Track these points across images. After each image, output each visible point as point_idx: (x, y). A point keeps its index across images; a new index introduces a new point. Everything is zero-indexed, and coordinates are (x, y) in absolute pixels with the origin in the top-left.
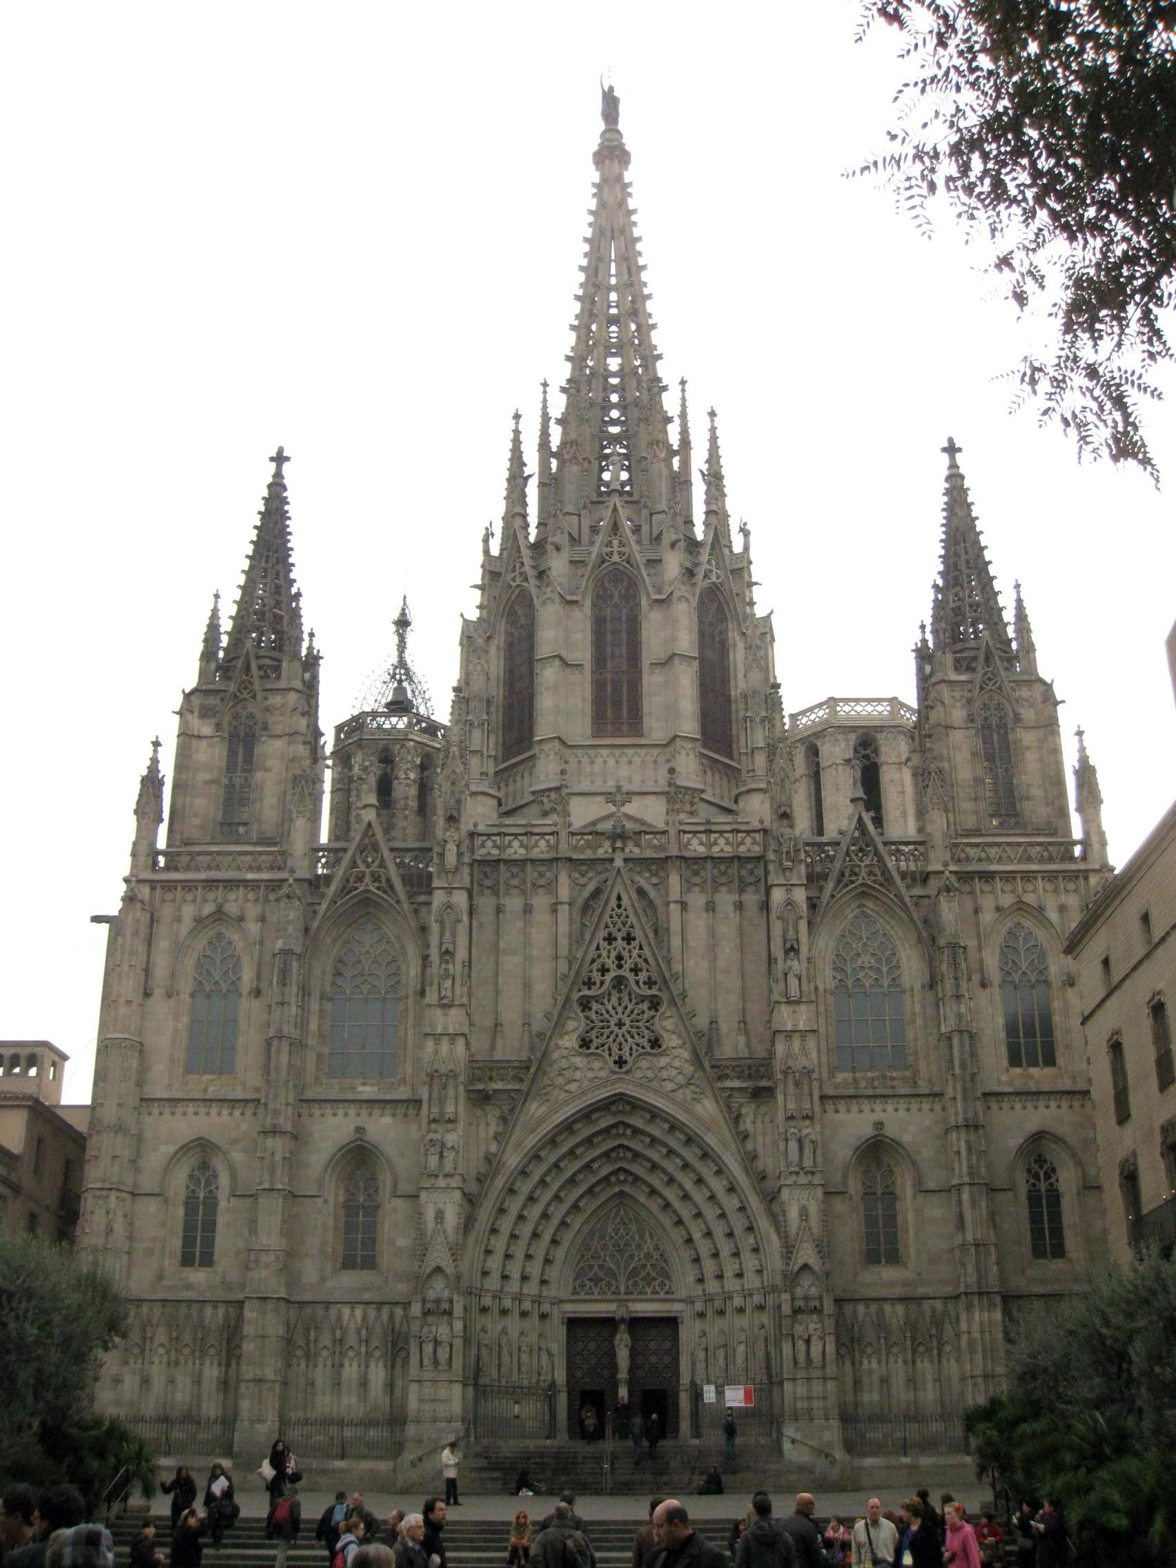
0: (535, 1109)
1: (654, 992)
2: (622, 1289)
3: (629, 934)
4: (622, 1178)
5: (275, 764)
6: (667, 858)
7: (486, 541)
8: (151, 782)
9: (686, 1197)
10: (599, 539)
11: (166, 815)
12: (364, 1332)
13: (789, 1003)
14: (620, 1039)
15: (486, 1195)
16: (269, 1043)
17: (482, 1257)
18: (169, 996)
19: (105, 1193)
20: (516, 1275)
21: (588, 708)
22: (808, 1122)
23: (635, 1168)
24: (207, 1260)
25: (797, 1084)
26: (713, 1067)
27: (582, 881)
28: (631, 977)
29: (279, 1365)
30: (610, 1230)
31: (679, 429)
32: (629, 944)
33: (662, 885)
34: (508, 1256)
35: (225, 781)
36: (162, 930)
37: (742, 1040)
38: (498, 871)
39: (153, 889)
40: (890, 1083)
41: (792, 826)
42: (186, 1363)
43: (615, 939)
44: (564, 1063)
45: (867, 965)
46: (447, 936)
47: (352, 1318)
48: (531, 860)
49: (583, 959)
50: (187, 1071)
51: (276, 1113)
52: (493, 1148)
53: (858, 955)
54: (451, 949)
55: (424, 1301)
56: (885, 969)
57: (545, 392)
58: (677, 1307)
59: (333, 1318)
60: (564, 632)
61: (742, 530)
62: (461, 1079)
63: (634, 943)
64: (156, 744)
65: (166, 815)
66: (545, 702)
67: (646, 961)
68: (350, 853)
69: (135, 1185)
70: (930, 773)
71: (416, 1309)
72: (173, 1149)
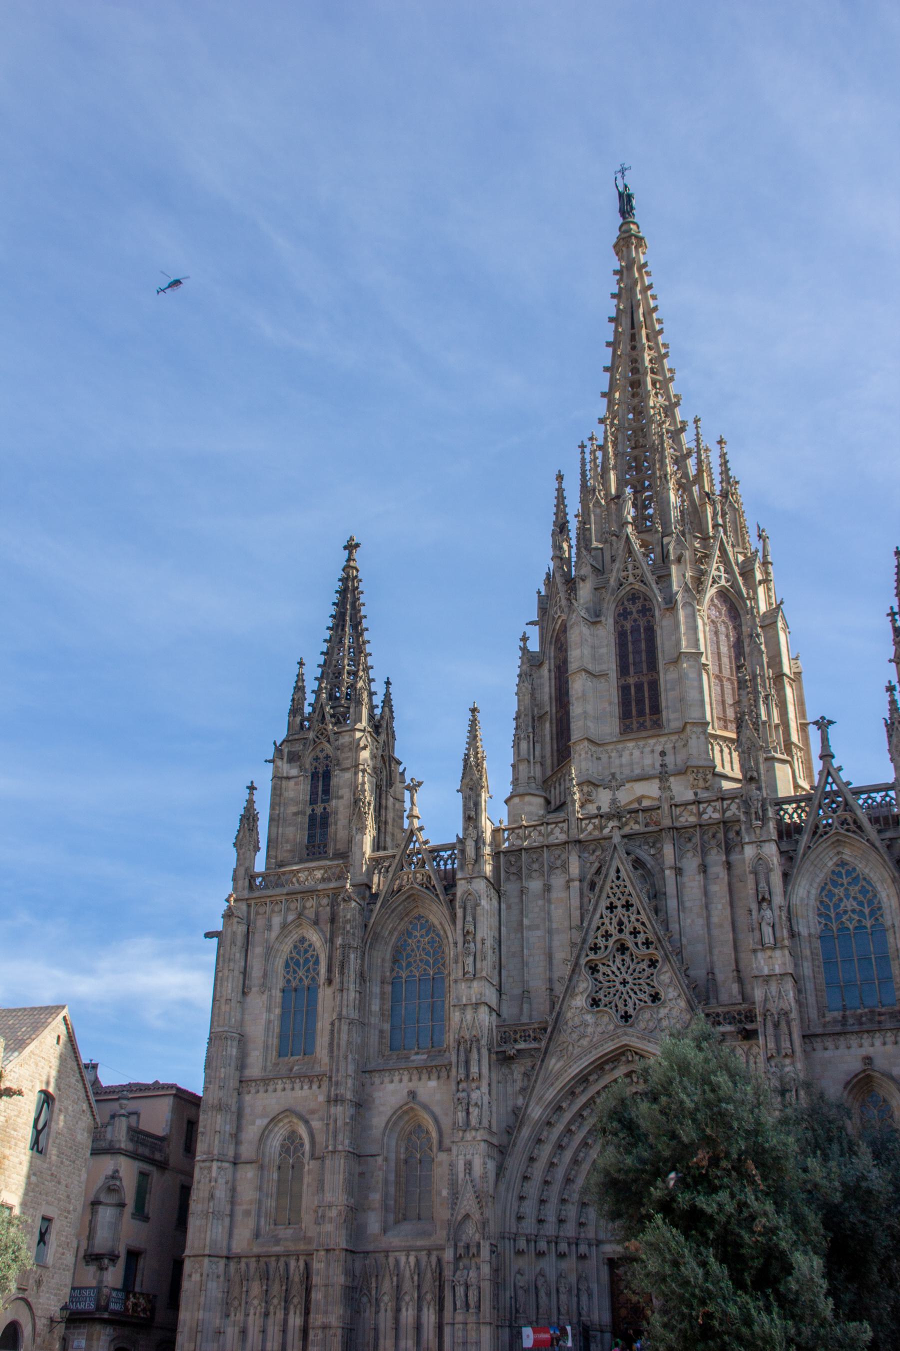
0: (554, 1064)
3: (627, 902)
5: (346, 793)
6: (661, 830)
8: (249, 818)
10: (617, 565)
11: (263, 844)
12: (416, 1278)
14: (625, 996)
15: (514, 1145)
16: (332, 1024)
17: (515, 1205)
19: (208, 1164)
20: (552, 1219)
21: (616, 710)
22: (787, 1061)
24: (293, 1219)
25: (776, 1025)
26: (707, 1015)
29: (341, 1312)
31: (696, 461)
32: (628, 910)
33: (658, 857)
34: (542, 1202)
35: (309, 811)
36: (257, 938)
37: (735, 987)
38: (520, 858)
39: (249, 906)
40: (877, 1018)
41: (759, 789)
42: (275, 1313)
43: (616, 907)
45: (849, 908)
46: (469, 918)
48: (547, 846)
49: (588, 928)
50: (280, 1055)
51: (337, 1083)
53: (841, 900)
54: (472, 929)
55: (456, 1246)
56: (867, 911)
57: (583, 452)
59: (392, 1268)
60: (593, 647)
61: (760, 536)
62: (483, 1042)
64: (252, 788)
65: (263, 844)
66: (576, 710)
67: (643, 924)
68: (397, 858)
69: (237, 1156)
71: (448, 1255)
72: (266, 1121)
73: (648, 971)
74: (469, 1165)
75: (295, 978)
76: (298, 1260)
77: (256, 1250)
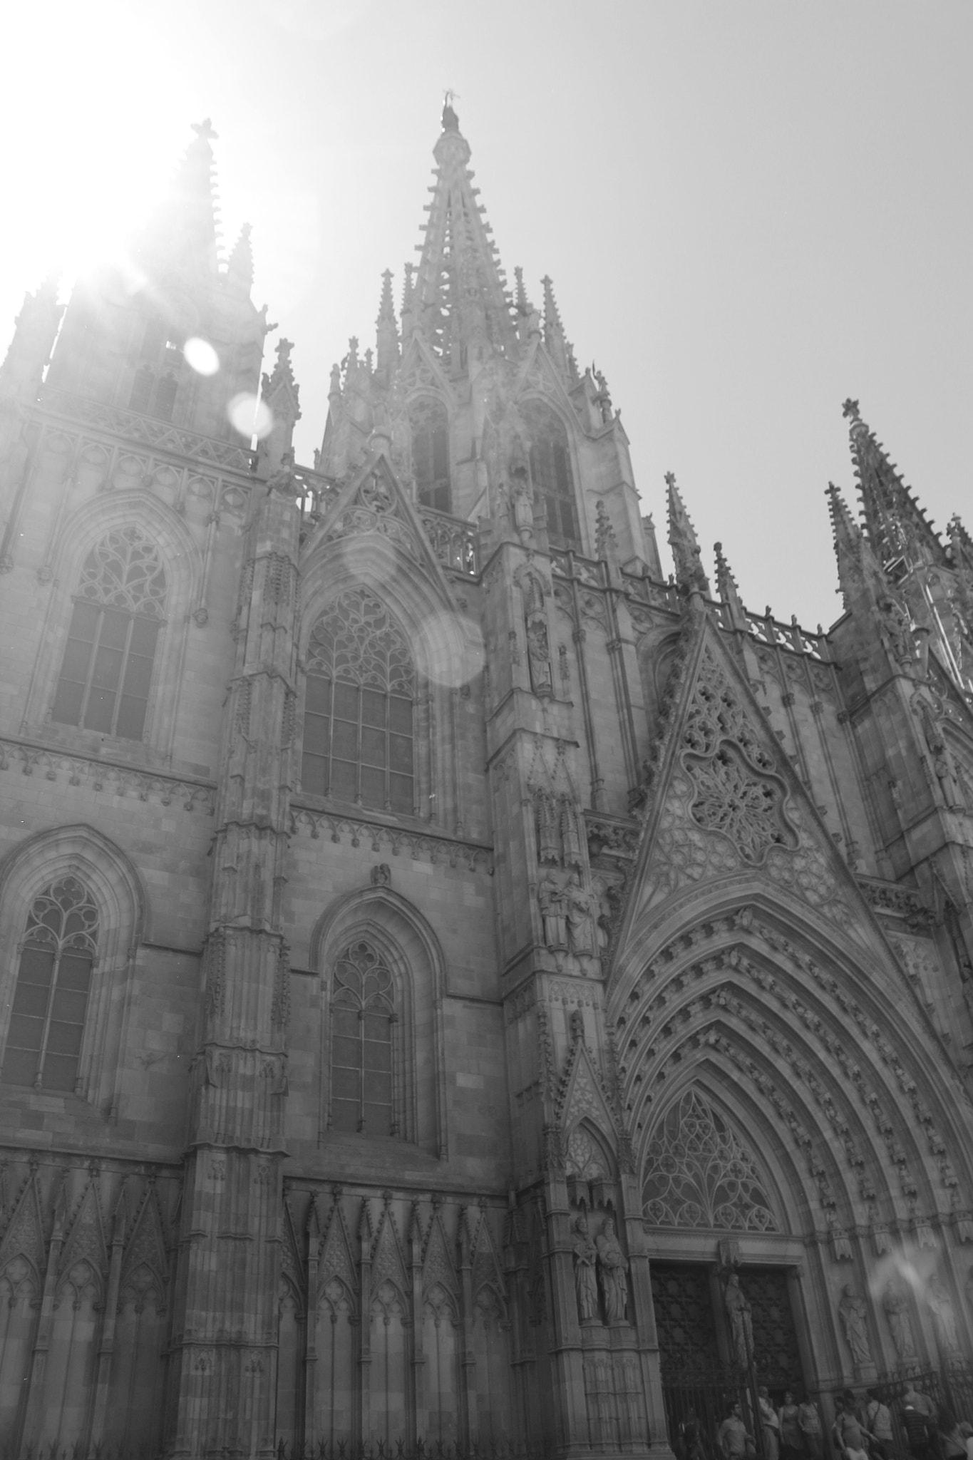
0: (649, 894)
1: (770, 771)
4: (712, 1040)
7: (335, 374)
18: (42, 582)
23: (734, 1023)
27: (642, 628)
28: (741, 745)
30: (682, 1122)
44: (678, 836)
55: (571, 1181)
58: (794, 1252)
73: (765, 802)
74: (575, 1022)
75: (107, 591)
76: (94, 1172)
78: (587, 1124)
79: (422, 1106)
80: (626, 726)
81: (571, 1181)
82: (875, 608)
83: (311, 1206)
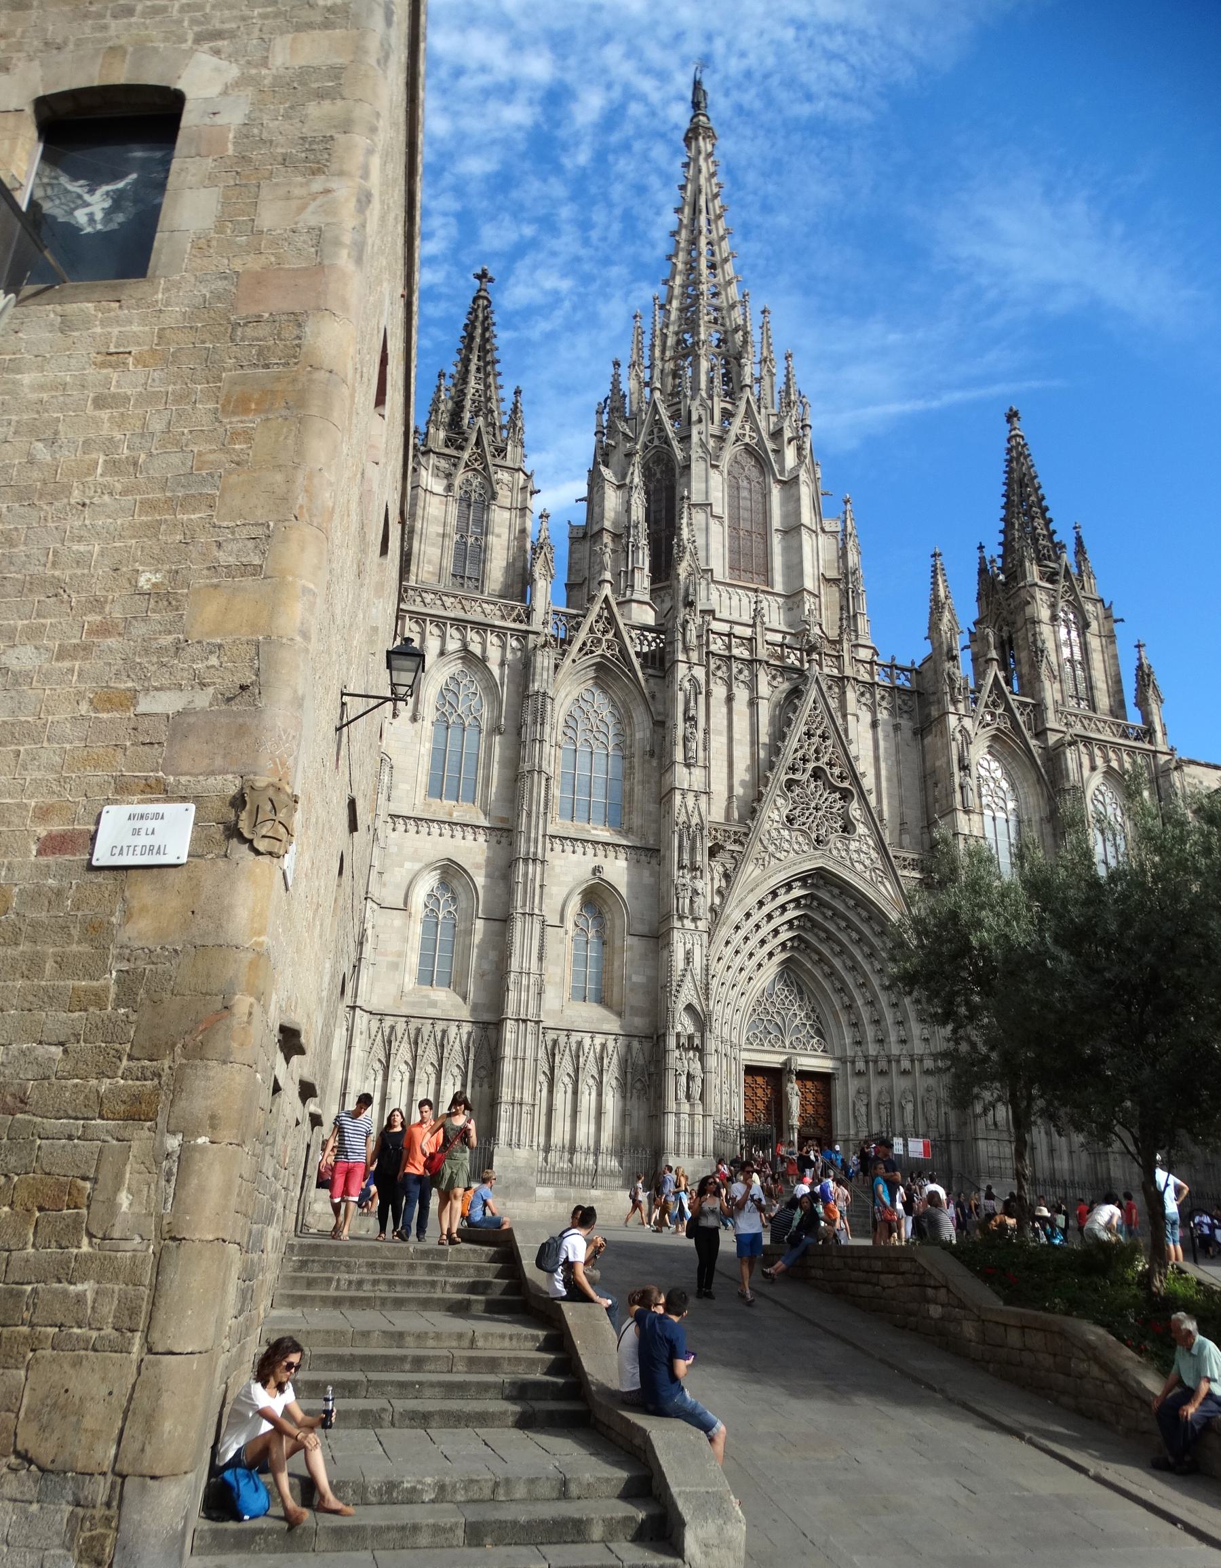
0: (750, 871)
1: (846, 785)
2: (787, 1044)
9: (854, 968)
13: (967, 811)
26: (895, 857)
27: (775, 683)
28: (827, 768)
47: (591, 1045)
52: (717, 900)
55: (678, 1035)
63: (828, 742)
70: (1042, 651)
72: (417, 866)
77: (405, 1011)
78: (689, 1008)
79: (616, 989)
80: (754, 756)
81: (678, 1035)
82: (945, 658)
83: (555, 1042)
